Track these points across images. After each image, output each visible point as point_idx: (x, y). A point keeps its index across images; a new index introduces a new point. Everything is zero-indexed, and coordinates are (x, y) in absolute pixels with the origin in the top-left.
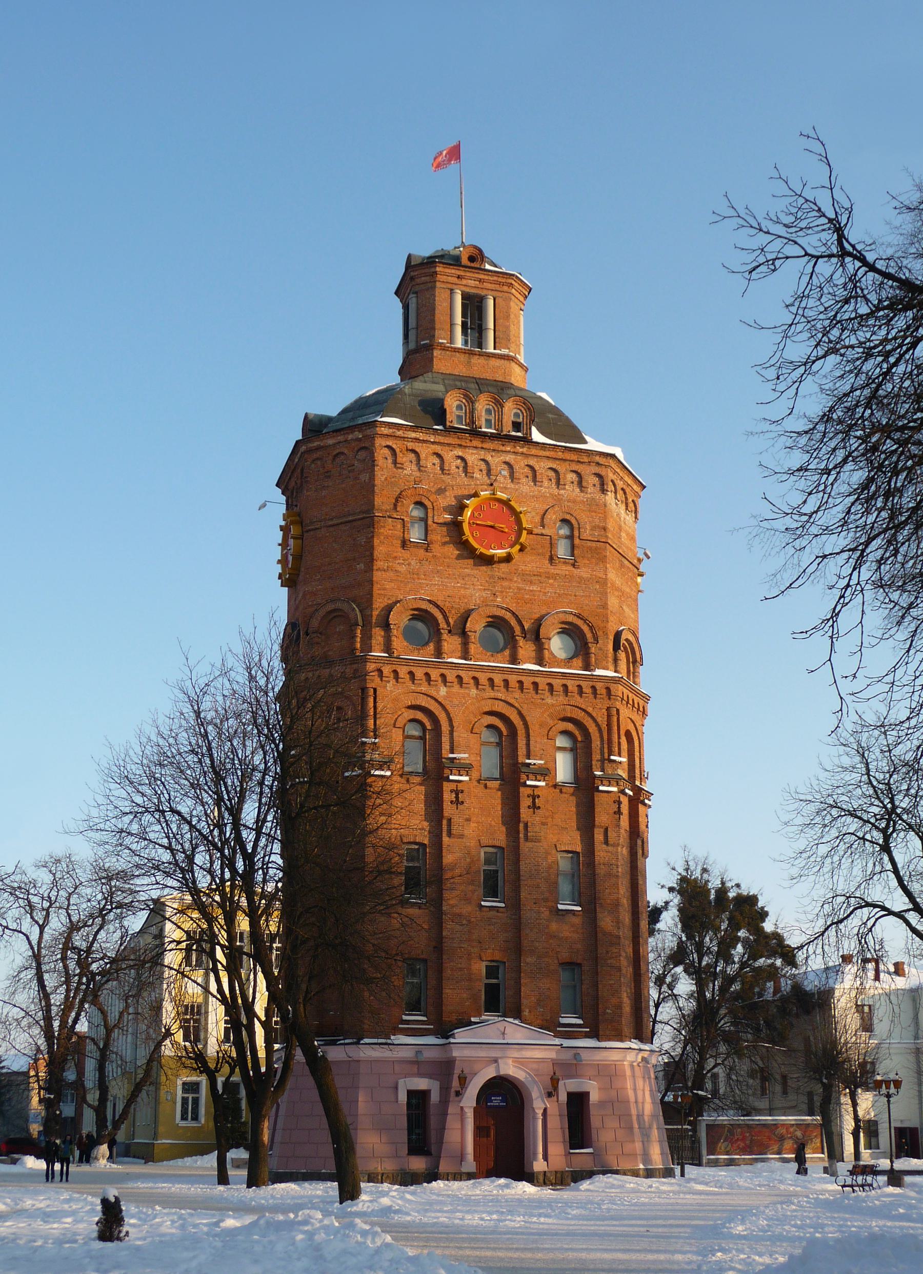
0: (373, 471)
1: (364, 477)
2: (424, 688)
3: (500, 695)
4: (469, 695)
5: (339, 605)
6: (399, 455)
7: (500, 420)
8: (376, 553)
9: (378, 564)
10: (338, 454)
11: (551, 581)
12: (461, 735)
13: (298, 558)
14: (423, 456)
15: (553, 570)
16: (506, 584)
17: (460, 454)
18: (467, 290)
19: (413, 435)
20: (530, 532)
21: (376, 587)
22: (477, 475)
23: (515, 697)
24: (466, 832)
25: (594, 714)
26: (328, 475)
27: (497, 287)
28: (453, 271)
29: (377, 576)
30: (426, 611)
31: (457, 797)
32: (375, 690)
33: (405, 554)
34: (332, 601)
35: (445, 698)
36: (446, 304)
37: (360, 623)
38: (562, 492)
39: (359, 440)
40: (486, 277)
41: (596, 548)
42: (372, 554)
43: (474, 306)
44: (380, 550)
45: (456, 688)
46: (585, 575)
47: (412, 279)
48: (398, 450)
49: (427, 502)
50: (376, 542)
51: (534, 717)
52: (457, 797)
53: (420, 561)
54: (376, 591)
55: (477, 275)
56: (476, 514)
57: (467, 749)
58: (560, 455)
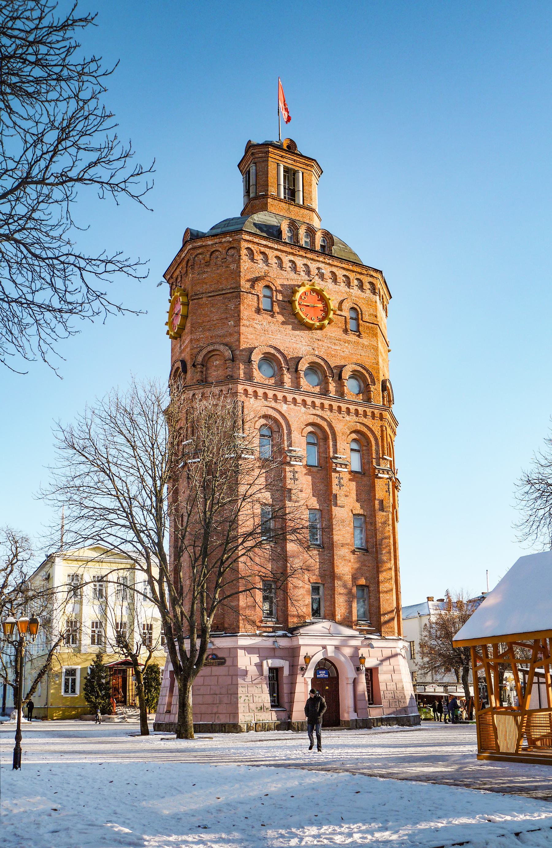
0: (239, 262)
1: (233, 266)
2: (273, 404)
4: (300, 410)
5: (217, 347)
9: (243, 322)
10: (214, 251)
11: (347, 345)
14: (270, 257)
15: (347, 338)
16: (320, 343)
17: (292, 259)
18: (287, 165)
19: (264, 243)
21: (242, 336)
23: (327, 414)
27: (304, 166)
28: (279, 152)
30: (273, 355)
34: (212, 344)
35: (286, 411)
36: (275, 172)
38: (351, 291)
39: (230, 242)
40: (299, 159)
42: (239, 316)
45: (292, 406)
46: (366, 343)
48: (255, 252)
50: (242, 307)
51: (339, 427)
55: (293, 157)
56: (303, 298)
58: (351, 267)
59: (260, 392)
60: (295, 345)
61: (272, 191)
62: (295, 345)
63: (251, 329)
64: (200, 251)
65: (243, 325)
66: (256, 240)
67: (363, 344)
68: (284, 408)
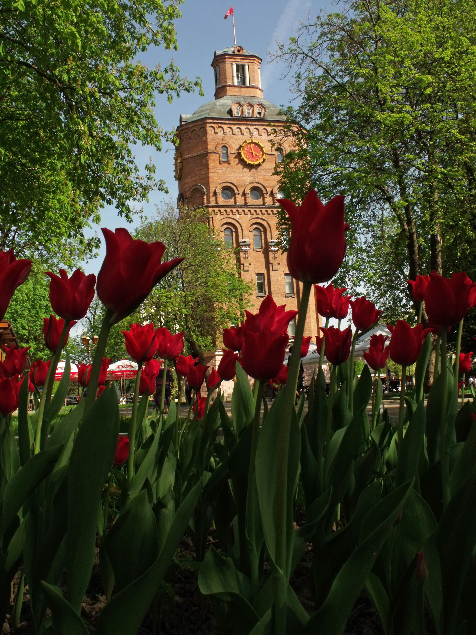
2: (231, 216)
3: (259, 216)
6: (216, 129)
7: (253, 112)
9: (211, 170)
12: (246, 232)
13: (181, 170)
14: (225, 128)
16: (259, 174)
20: (267, 154)
21: (210, 179)
22: (245, 134)
24: (250, 269)
26: (190, 138)
29: (211, 175)
33: (221, 166)
36: (230, 69)
37: (206, 193)
43: (241, 69)
44: (211, 165)
47: (217, 60)
49: (227, 146)
50: (209, 162)
54: (211, 180)
57: (249, 237)
59: (222, 210)
61: (229, 82)
63: (216, 174)
64: (186, 131)
66: (215, 121)
68: (237, 217)
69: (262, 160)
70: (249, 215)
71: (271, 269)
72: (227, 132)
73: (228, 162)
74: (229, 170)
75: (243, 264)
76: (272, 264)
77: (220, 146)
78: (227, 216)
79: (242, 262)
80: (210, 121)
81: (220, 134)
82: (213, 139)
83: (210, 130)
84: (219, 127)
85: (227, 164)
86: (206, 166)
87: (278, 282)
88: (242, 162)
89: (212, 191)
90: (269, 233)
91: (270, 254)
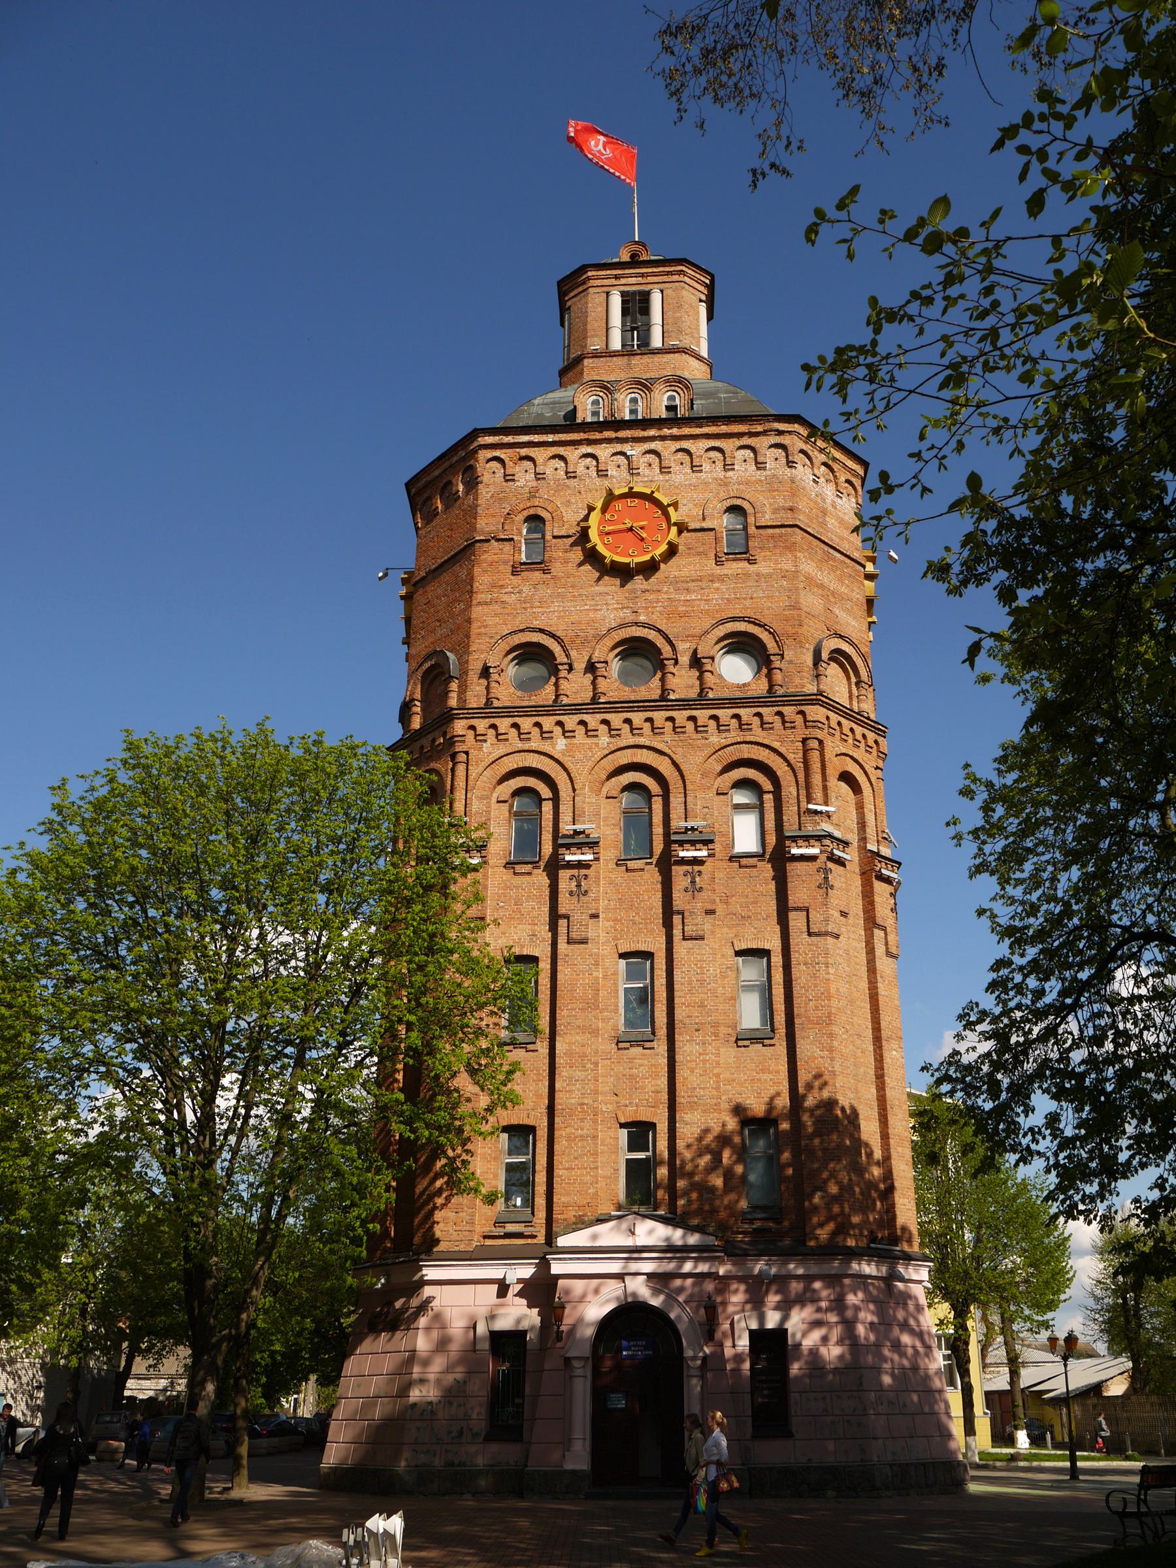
4: (597, 745)
6: (508, 463)
8: (476, 585)
11: (716, 585)
12: (588, 799)
15: (718, 571)
16: (652, 597)
21: (475, 625)
25: (782, 750)
29: (477, 612)
31: (579, 886)
32: (467, 753)
33: (515, 580)
35: (563, 753)
38: (730, 473)
41: (781, 536)
44: (482, 580)
52: (579, 886)
53: (535, 586)
54: (475, 629)
58: (724, 429)
60: (591, 615)
62: (591, 615)
65: (479, 603)
67: (758, 575)
68: (560, 745)
69: (664, 547)
70: (604, 740)
71: (677, 933)
72: (549, 471)
73: (540, 565)
74: (545, 592)
75: (567, 917)
76: (682, 913)
77: (521, 517)
78: (520, 745)
79: (562, 910)
80: (489, 440)
81: (524, 477)
82: (498, 498)
83: (489, 474)
84: (522, 458)
85: (538, 574)
86: (467, 588)
87: (702, 982)
88: (592, 557)
89: (475, 666)
90: (676, 801)
91: (678, 871)
